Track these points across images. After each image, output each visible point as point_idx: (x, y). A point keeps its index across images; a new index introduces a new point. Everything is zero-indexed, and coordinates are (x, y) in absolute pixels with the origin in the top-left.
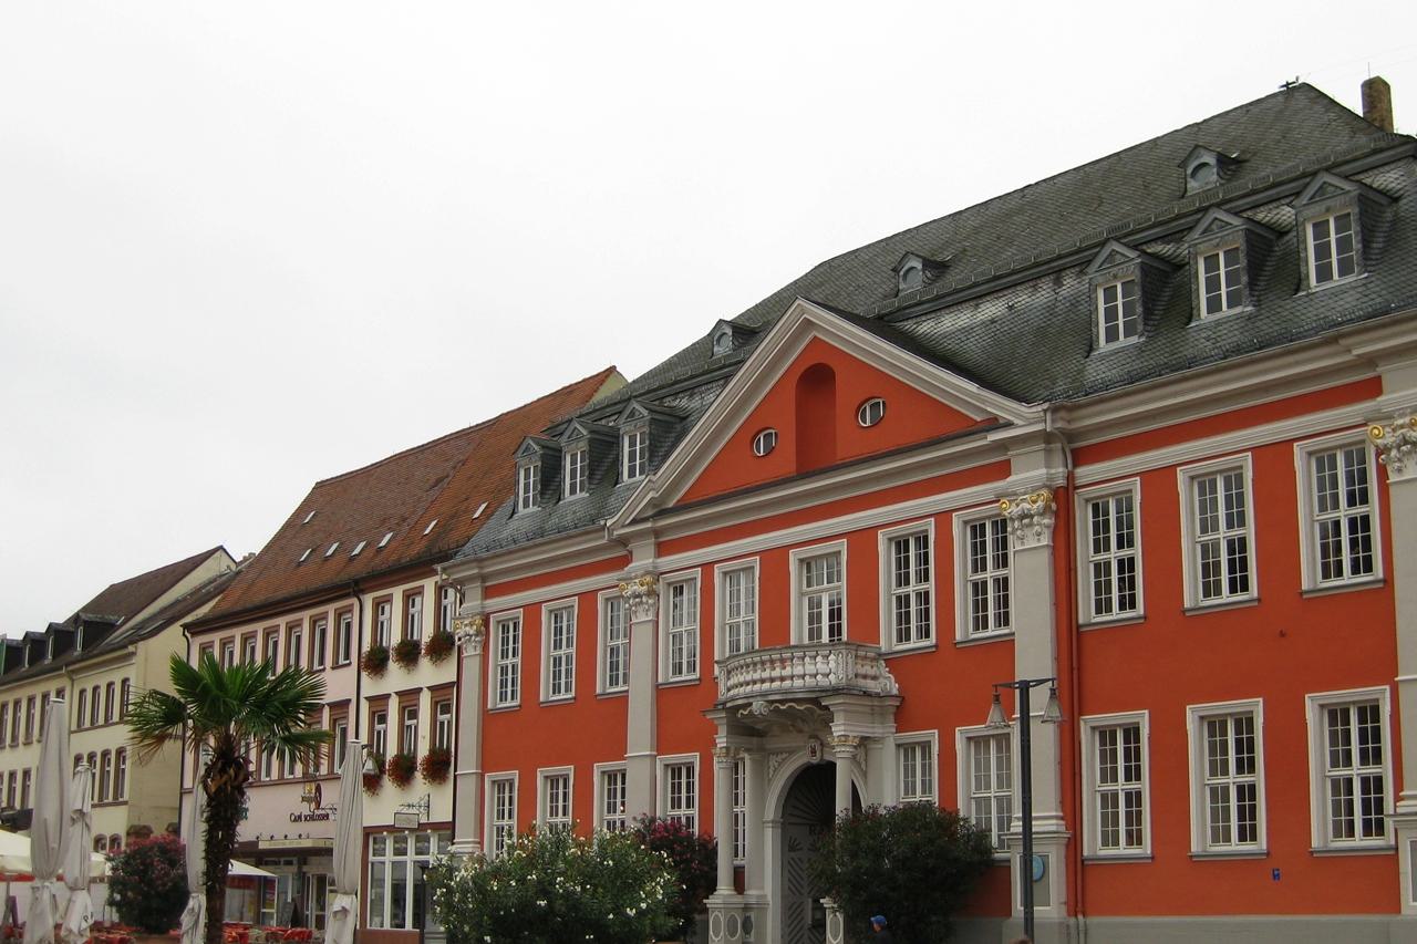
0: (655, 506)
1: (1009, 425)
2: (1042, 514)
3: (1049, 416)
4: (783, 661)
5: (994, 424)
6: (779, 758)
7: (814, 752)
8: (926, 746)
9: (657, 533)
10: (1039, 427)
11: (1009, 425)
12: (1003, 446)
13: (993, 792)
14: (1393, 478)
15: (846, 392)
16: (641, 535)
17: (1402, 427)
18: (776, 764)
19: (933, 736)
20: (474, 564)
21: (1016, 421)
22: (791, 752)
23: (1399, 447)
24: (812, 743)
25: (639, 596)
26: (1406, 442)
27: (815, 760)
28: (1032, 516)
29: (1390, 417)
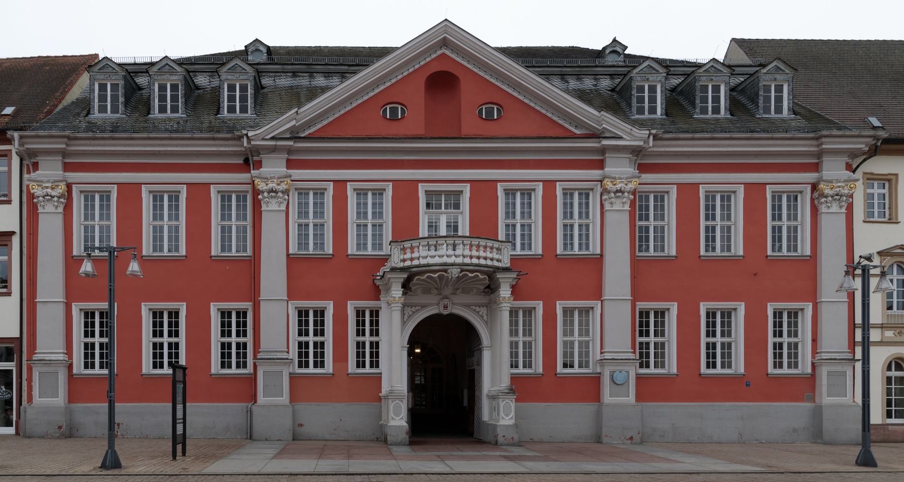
0: (292, 132)
1: (620, 138)
2: (629, 192)
3: (651, 138)
4: (412, 248)
5: (596, 135)
6: (413, 309)
7: (446, 307)
8: (529, 312)
9: (290, 151)
10: (641, 143)
11: (620, 138)
12: (603, 151)
13: (576, 337)
14: (823, 209)
15: (468, 94)
16: (274, 150)
17: (839, 187)
18: (411, 313)
19: (539, 306)
20: (65, 140)
21: (624, 137)
22: (424, 306)
23: (832, 197)
24: (446, 302)
25: (276, 192)
26: (837, 195)
27: (445, 312)
28: (623, 192)
29: (831, 182)
